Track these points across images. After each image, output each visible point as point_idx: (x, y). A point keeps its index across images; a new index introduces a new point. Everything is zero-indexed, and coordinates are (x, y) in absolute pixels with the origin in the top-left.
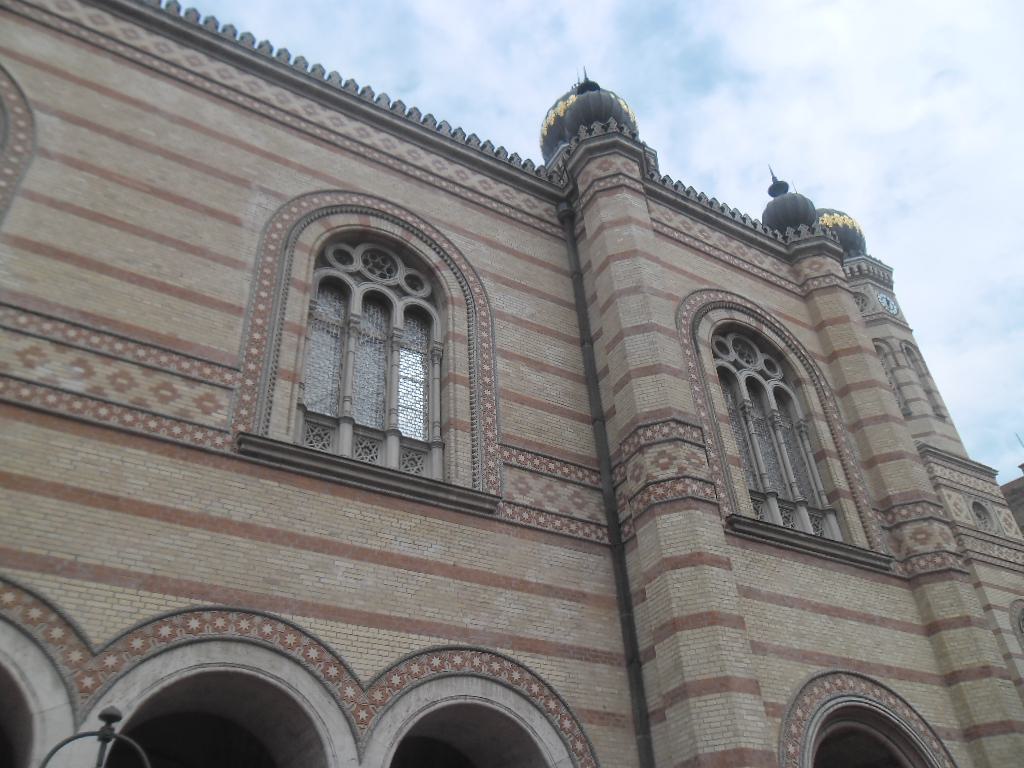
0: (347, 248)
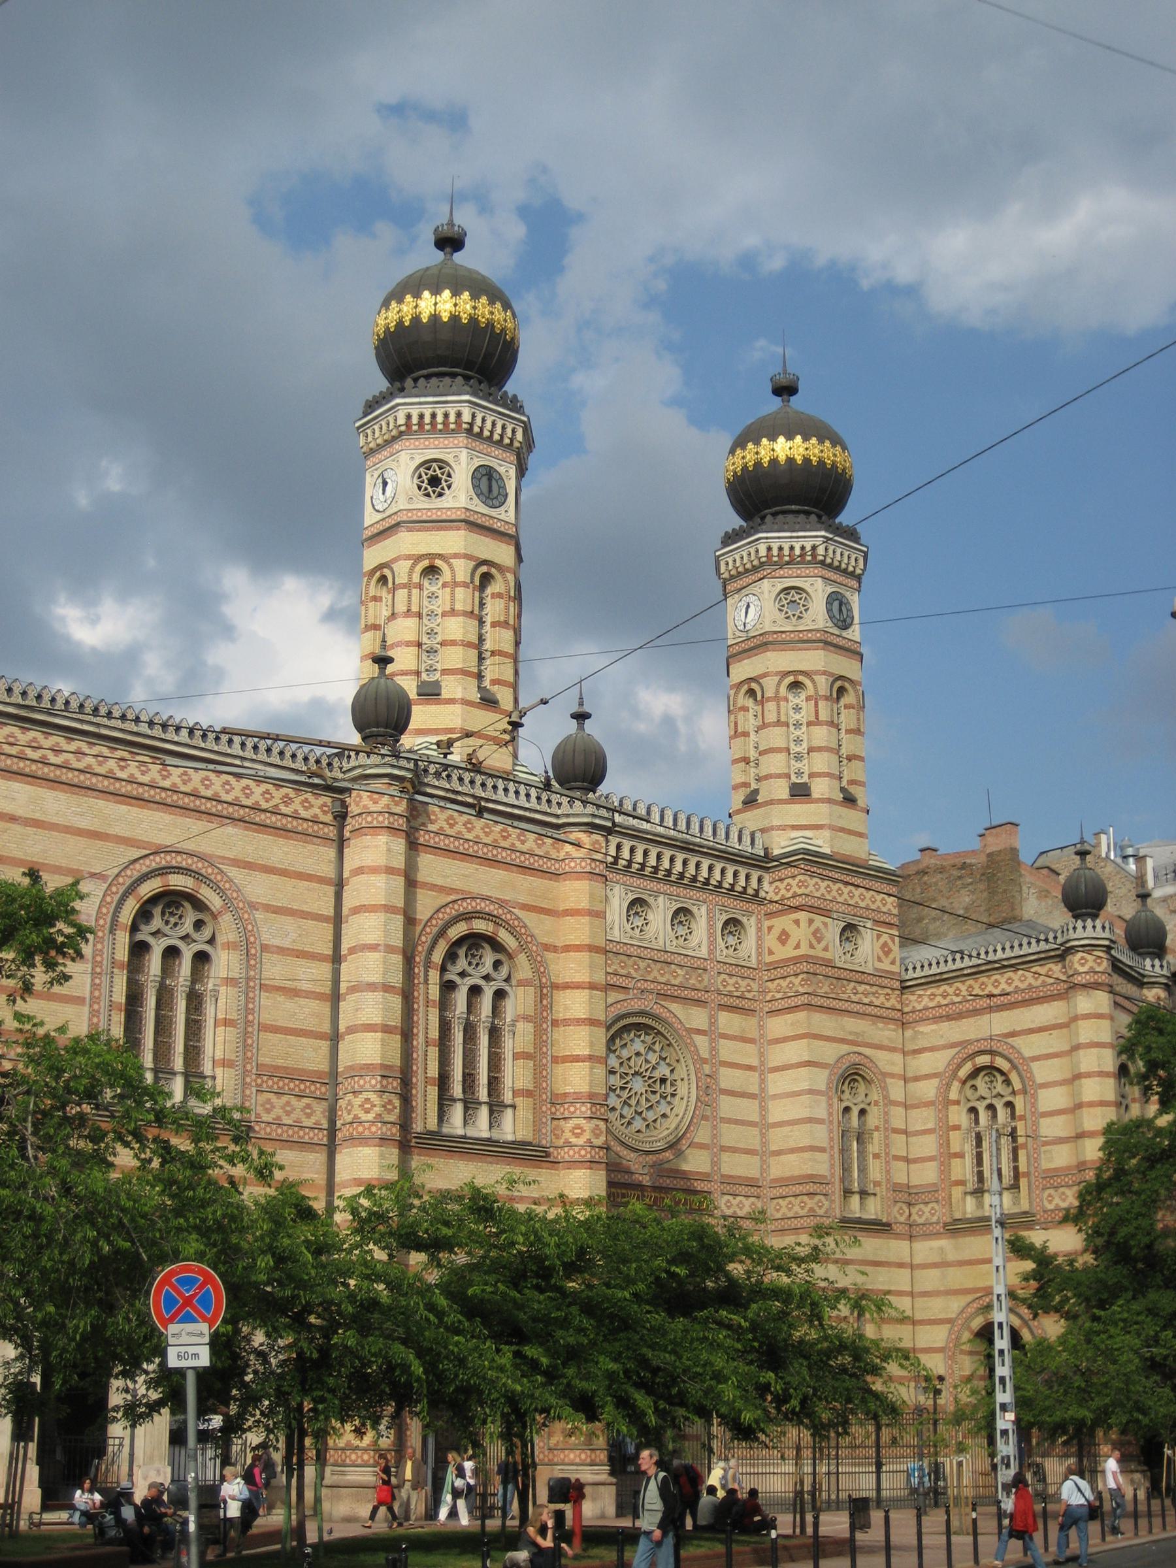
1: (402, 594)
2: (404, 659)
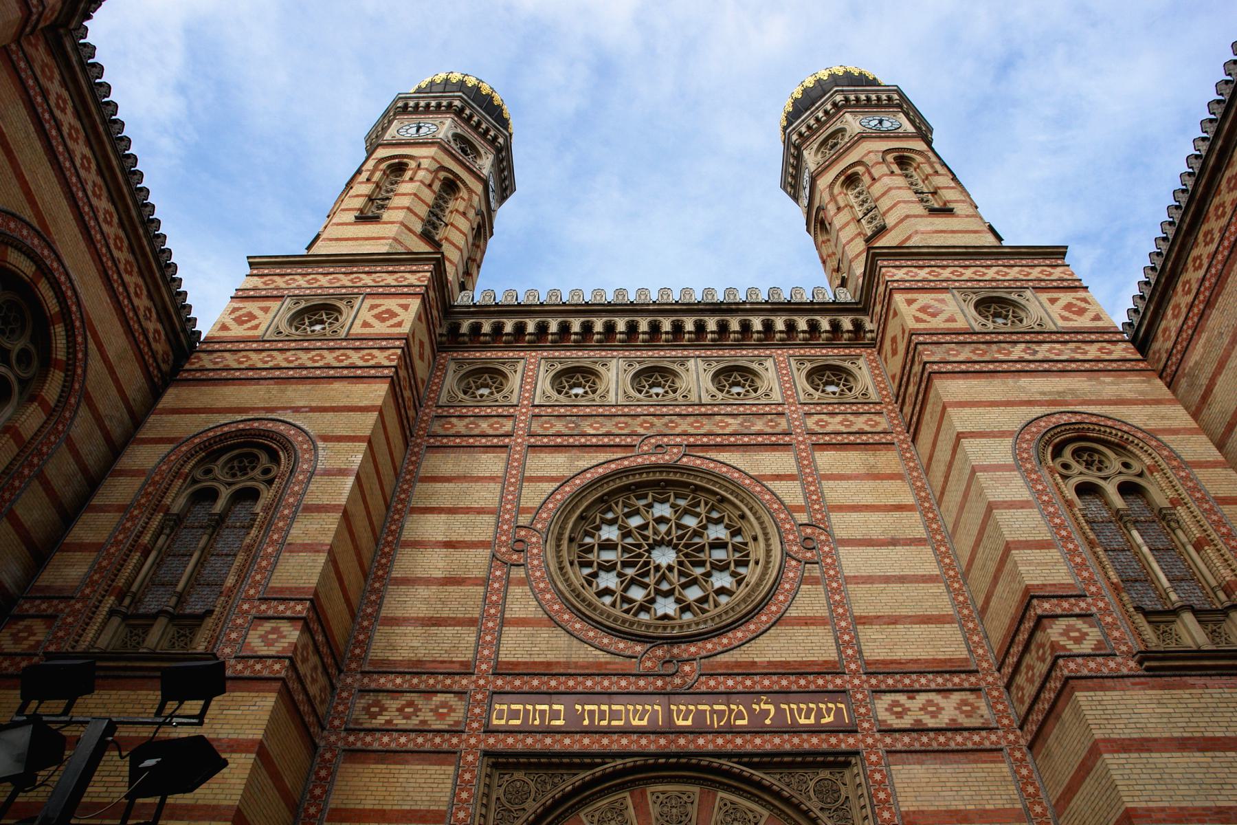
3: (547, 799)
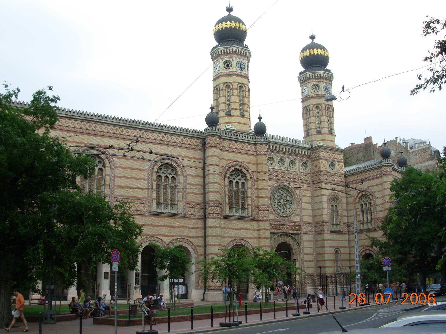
0: (160, 167)
1: (221, 92)
2: (222, 107)
3: (274, 237)
